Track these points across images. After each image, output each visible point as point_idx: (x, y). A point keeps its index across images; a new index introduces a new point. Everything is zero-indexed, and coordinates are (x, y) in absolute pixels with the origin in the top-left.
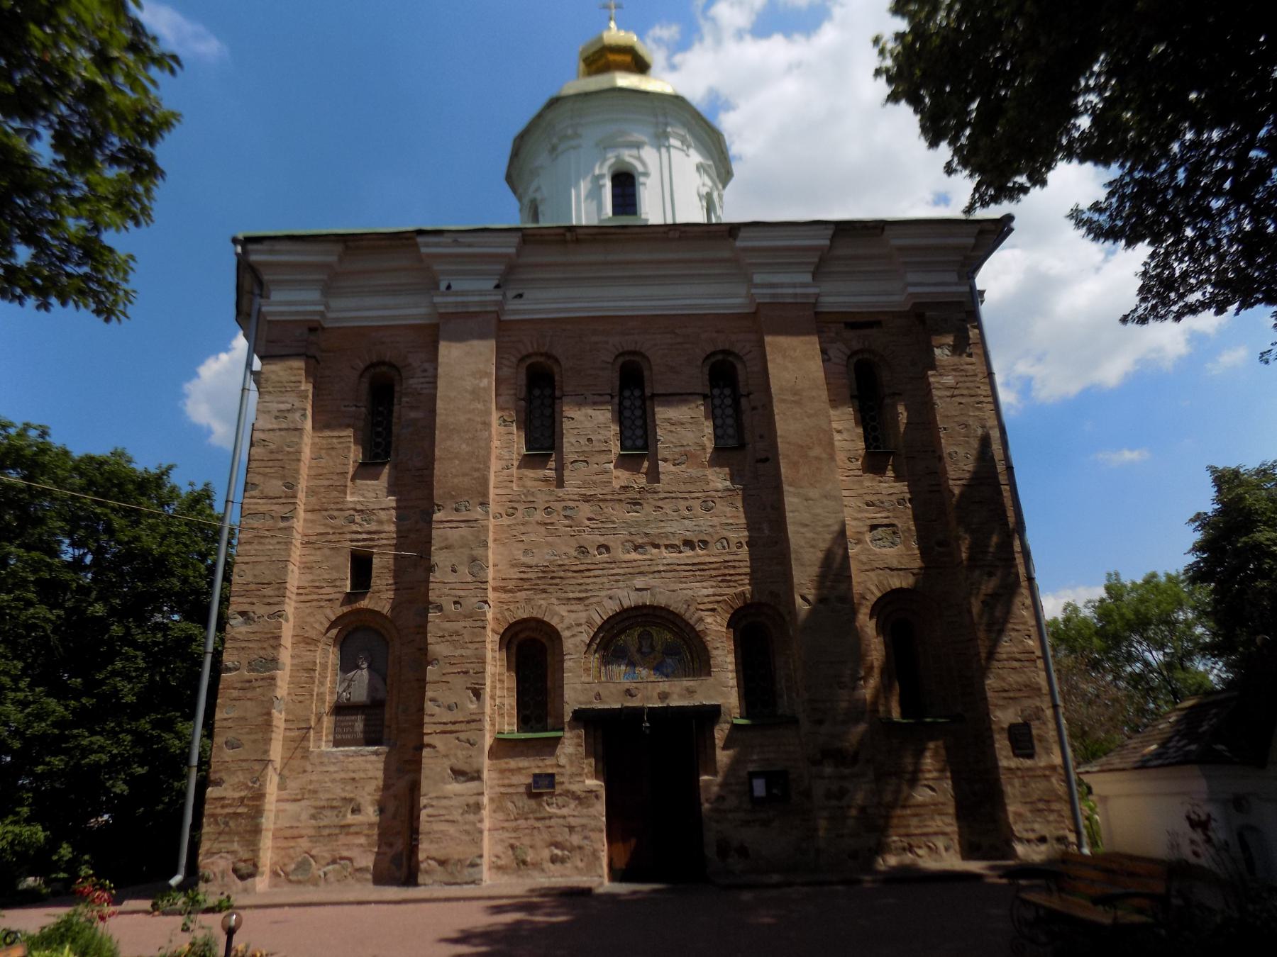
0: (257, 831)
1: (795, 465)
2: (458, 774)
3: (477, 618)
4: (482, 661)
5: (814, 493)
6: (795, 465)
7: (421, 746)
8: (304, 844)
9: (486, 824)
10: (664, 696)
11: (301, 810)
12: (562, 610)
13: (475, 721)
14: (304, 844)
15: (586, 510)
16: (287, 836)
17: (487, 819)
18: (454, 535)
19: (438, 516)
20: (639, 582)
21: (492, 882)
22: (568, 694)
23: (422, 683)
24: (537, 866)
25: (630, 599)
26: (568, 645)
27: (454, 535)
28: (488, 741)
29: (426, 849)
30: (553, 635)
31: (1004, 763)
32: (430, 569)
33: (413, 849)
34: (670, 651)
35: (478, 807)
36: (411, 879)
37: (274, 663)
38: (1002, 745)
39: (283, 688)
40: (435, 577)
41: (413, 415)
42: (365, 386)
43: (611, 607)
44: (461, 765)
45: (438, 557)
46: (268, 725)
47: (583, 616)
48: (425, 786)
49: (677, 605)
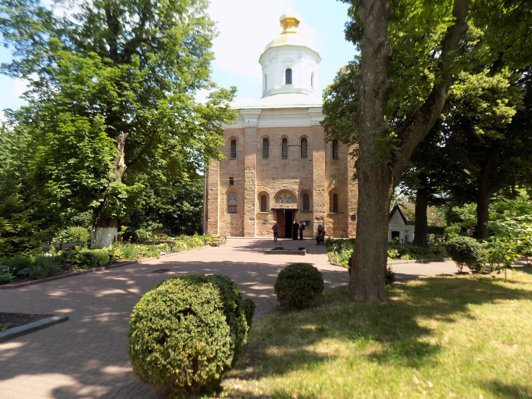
0: (217, 227)
1: (316, 163)
2: (251, 219)
3: (253, 191)
4: (255, 199)
5: (319, 169)
6: (316, 163)
7: (244, 214)
8: (224, 229)
9: (256, 228)
10: (288, 207)
11: (224, 224)
12: (269, 190)
13: (253, 210)
14: (224, 229)
15: (274, 169)
16: (222, 228)
17: (256, 226)
18: (249, 175)
19: (246, 171)
20: (284, 185)
21: (256, 236)
22: (270, 205)
23: (244, 203)
24: (264, 235)
25: (283, 188)
26: (271, 196)
27: (249, 175)
28: (256, 213)
29: (245, 231)
30: (268, 194)
31: (349, 221)
32: (245, 181)
33: (243, 231)
34: (290, 198)
35: (254, 224)
36: (243, 235)
37: (217, 198)
38: (349, 218)
39: (219, 203)
40: (246, 183)
41: (240, 149)
42: (230, 142)
43: (279, 190)
44: (251, 217)
45: (246, 179)
46: (217, 209)
47: (273, 191)
48: (245, 221)
49: (292, 190)
